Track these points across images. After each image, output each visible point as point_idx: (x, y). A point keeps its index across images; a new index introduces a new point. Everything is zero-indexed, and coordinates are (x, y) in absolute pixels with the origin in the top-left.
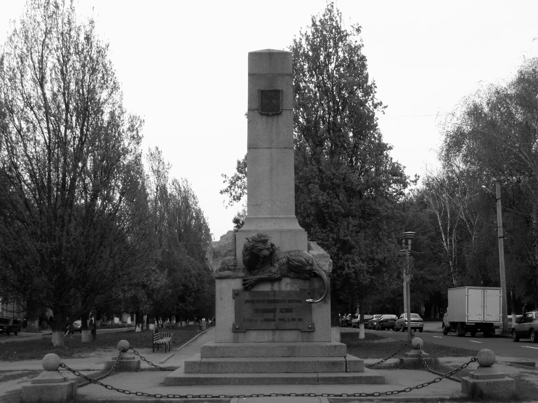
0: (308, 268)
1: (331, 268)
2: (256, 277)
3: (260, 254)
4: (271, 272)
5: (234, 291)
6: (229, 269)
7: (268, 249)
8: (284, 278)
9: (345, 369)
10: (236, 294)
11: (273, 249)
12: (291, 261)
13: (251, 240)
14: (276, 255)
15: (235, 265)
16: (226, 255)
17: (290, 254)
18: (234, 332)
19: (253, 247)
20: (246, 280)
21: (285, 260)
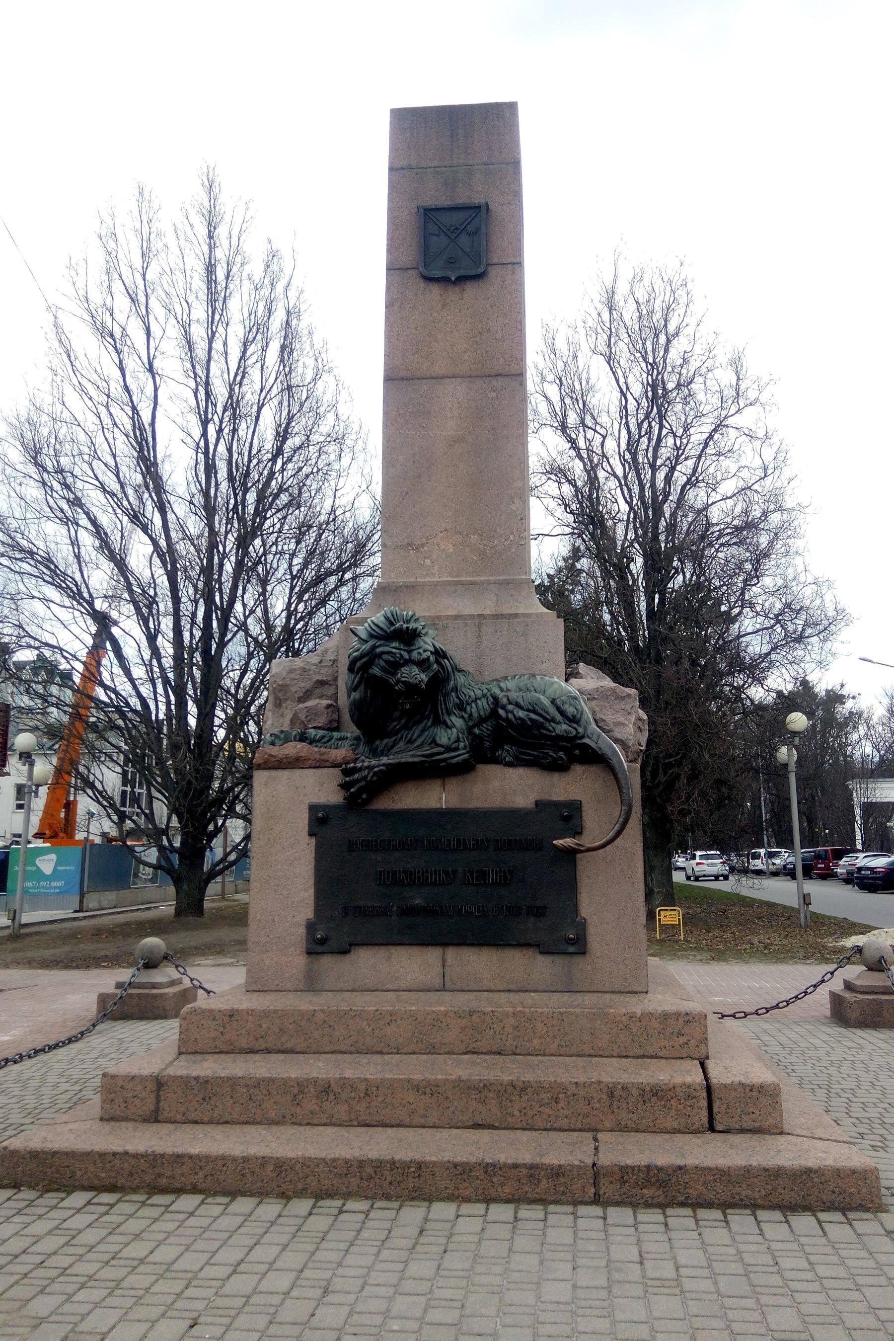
0: (563, 728)
1: (644, 738)
2: (385, 760)
3: (392, 681)
4: (434, 742)
5: (313, 808)
6: (302, 738)
7: (423, 664)
8: (480, 767)
9: (705, 1120)
10: (320, 820)
11: (441, 673)
12: (504, 708)
13: (364, 635)
14: (455, 689)
15: (334, 726)
16: (307, 695)
17: (502, 685)
18: (309, 953)
19: (371, 656)
20: (355, 770)
21: (483, 704)
